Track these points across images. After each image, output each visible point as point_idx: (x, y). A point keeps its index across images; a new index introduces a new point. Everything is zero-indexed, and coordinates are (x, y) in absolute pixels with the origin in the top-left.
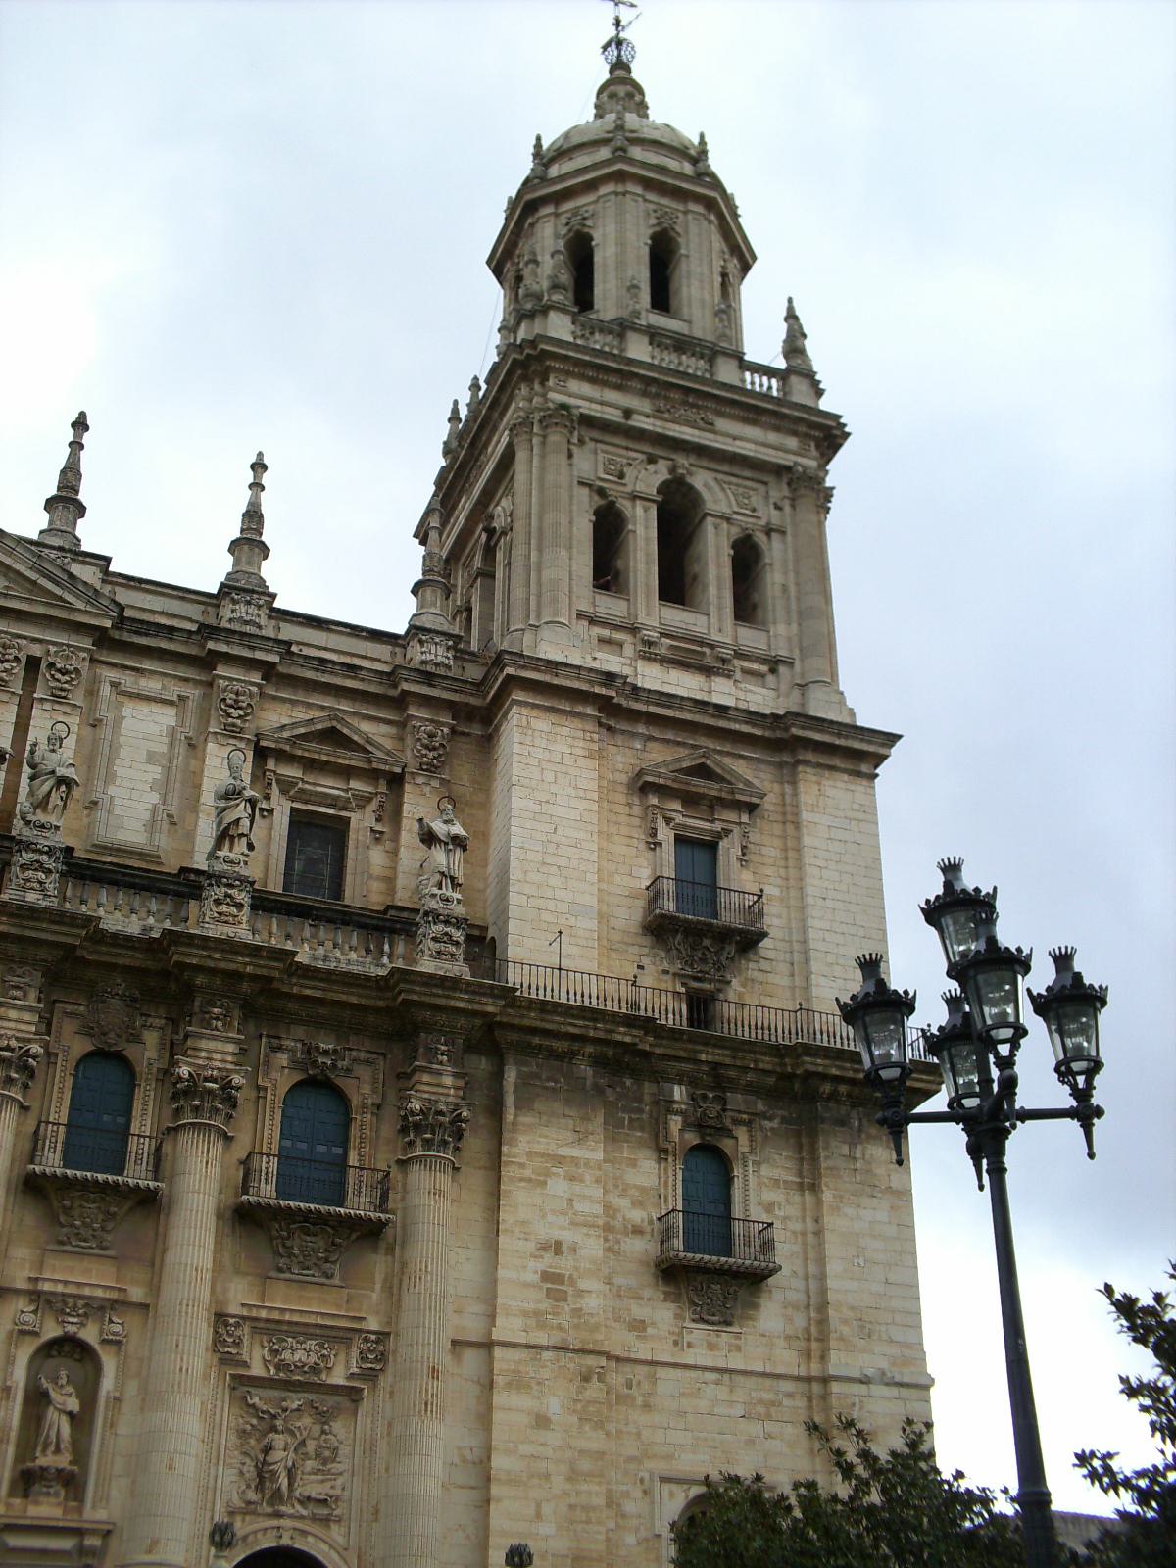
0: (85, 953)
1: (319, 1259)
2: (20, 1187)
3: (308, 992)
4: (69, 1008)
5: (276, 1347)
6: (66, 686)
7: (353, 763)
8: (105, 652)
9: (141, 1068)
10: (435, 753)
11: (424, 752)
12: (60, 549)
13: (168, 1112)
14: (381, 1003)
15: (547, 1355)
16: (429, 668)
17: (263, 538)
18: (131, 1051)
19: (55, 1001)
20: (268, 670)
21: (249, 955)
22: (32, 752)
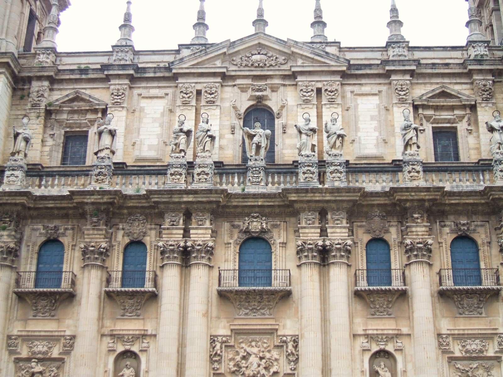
0: (361, 202)
1: (475, 307)
2: (353, 296)
3: (453, 202)
4: (359, 224)
5: (463, 344)
6: (333, 97)
7: (454, 104)
8: (346, 80)
9: (391, 243)
10: (488, 92)
11: (483, 93)
12: (320, 43)
13: (405, 258)
14: (483, 201)
16: (479, 58)
17: (400, 19)
18: (386, 237)
19: (353, 222)
20: (412, 73)
21: (426, 191)
22: (326, 127)
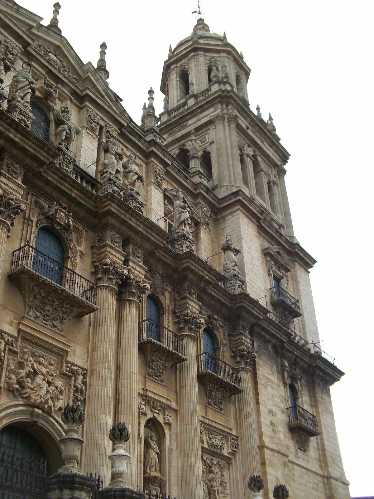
14: (230, 305)
15: (276, 454)
18: (161, 298)
